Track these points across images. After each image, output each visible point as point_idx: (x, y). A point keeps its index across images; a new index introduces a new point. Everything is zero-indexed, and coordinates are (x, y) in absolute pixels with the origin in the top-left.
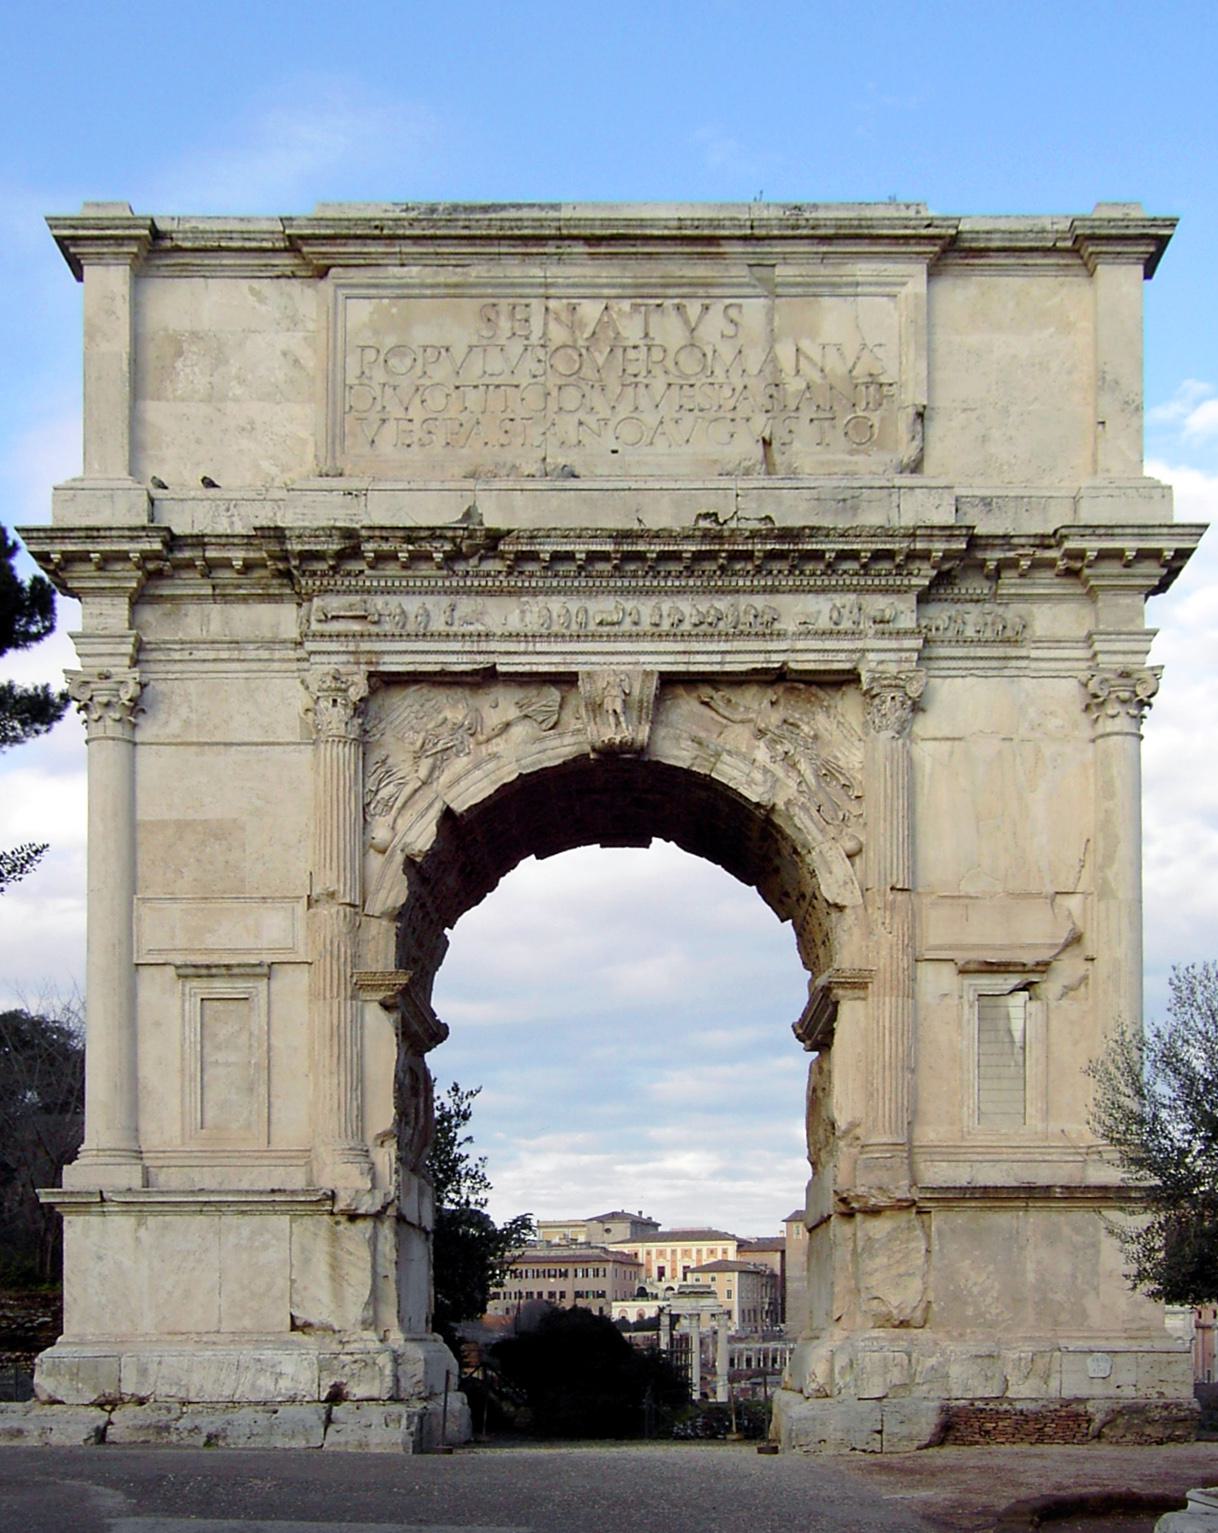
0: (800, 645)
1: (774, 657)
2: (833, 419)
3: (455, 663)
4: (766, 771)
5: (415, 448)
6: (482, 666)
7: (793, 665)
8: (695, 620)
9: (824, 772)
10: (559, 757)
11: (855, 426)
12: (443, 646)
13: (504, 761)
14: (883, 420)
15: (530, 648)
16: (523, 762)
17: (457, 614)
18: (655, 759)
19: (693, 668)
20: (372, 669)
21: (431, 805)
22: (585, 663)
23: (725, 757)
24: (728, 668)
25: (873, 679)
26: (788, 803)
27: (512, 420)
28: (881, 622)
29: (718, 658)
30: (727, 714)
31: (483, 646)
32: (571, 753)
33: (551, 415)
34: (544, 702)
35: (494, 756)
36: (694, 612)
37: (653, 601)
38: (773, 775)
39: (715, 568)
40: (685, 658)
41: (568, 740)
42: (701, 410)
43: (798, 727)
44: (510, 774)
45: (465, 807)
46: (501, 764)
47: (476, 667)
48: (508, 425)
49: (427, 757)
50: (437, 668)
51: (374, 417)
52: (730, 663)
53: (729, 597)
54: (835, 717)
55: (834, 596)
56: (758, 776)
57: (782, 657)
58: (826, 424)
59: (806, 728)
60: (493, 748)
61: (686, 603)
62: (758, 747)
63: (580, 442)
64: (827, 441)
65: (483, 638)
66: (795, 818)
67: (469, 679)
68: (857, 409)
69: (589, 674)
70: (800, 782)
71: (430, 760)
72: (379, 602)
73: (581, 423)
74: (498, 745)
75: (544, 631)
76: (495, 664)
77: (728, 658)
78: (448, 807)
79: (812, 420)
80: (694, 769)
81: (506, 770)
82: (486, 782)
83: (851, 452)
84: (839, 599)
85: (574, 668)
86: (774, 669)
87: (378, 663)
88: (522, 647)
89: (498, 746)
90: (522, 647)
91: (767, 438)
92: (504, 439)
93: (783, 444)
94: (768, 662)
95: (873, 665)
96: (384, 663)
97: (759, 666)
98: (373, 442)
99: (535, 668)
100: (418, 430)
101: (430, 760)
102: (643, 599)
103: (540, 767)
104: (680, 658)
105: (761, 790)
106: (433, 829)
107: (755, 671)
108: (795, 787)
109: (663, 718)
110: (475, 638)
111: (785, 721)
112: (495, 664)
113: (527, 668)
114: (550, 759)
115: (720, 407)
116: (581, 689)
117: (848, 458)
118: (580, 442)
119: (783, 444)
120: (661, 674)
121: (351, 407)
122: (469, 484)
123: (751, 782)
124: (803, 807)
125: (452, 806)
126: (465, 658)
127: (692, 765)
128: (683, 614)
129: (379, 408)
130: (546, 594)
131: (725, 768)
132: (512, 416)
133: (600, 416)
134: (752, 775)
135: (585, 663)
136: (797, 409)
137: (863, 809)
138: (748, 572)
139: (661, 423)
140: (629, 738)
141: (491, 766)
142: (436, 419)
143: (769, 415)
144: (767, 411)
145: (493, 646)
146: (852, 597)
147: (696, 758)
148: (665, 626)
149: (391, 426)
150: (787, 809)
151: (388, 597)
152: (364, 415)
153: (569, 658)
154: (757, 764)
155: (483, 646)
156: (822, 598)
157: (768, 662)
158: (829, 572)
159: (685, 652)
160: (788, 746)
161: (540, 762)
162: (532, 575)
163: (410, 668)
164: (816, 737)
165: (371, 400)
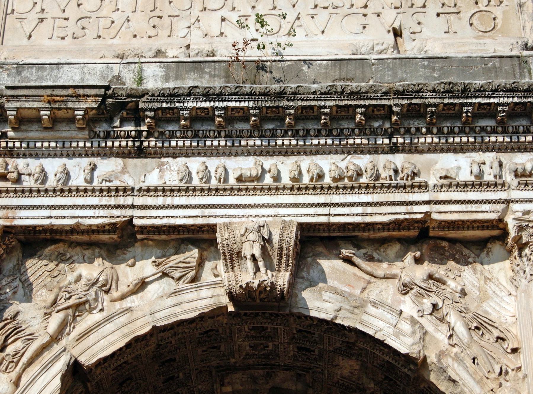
0: (443, 196)
1: (416, 208)
2: (458, 13)
3: (91, 217)
4: (413, 322)
5: (69, 39)
6: (118, 219)
7: (435, 216)
8: (336, 174)
9: (475, 324)
10: (195, 309)
11: (479, 19)
12: (80, 201)
13: (135, 315)
14: (504, 12)
15: (169, 201)
16: (156, 315)
17: (96, 174)
18: (295, 311)
19: (334, 220)
20: (8, 224)
21: (57, 357)
22: (223, 217)
23: (370, 309)
24: (368, 219)
25: (521, 229)
26: (441, 354)
27: (160, 17)
28: (523, 175)
29: (359, 210)
30: (369, 269)
31: (121, 201)
32: (207, 307)
33: (196, 12)
34: (182, 259)
35: (129, 310)
36: (333, 167)
37: (291, 160)
38: (422, 327)
39: (352, 126)
40: (325, 210)
41: (205, 293)
42: (336, 7)
43: (444, 283)
44: (142, 327)
45: (94, 361)
46: (134, 317)
47: (114, 221)
48: (156, 21)
49: (58, 312)
50: (71, 222)
51: (34, 17)
52: (371, 214)
53: (368, 156)
54: (482, 273)
55: (474, 154)
56: (406, 327)
57: (425, 208)
58: (453, 17)
59: (452, 284)
60: (127, 303)
61: (326, 161)
62: (404, 302)
63: (222, 34)
64: (454, 29)
65: (121, 193)
66: (449, 370)
67: (105, 237)
68: (480, 5)
69: (227, 225)
70: (451, 336)
71: (61, 315)
72: (21, 163)
73: (223, 20)
74: (133, 301)
75: (183, 185)
76: (132, 218)
77: (369, 210)
78: (76, 361)
79: (438, 15)
80: (338, 321)
81: (139, 323)
82: (117, 335)
83: (478, 38)
84: (478, 156)
85: (212, 221)
86: (417, 221)
87: (13, 218)
88: (160, 201)
89: (133, 301)
90: (160, 201)
91: (396, 25)
92: (152, 32)
93: (414, 33)
94: (410, 213)
95: (520, 215)
96: (20, 218)
97: (402, 217)
98: (30, 36)
99: (172, 222)
100: (72, 27)
101: (61, 315)
102: (281, 158)
103: (175, 320)
104: (320, 210)
105: (409, 341)
106: (57, 382)
107: (397, 224)
108: (446, 341)
109: (304, 274)
110: (113, 193)
111: (431, 277)
112: (132, 218)
113: (165, 222)
114: (185, 312)
115: (352, 5)
116: (219, 240)
117: (475, 41)
118: (222, 34)
119: (414, 33)
120: (301, 226)
121: (13, 10)
122: (118, 60)
123: (399, 333)
124: (457, 358)
125: (78, 359)
126: (102, 212)
127: (336, 317)
128: (322, 171)
129: (38, 8)
130: (187, 155)
131: (371, 320)
132: (160, 15)
133: (241, 13)
134: (399, 326)
135: (223, 217)
136: (424, 6)
137: (520, 360)
138: (386, 130)
139: (298, 18)
140: (268, 282)
141: (123, 319)
142: (90, 18)
143: (398, 11)
144: (396, 8)
145: (129, 201)
146: (493, 155)
147: (340, 310)
148: (306, 180)
149: (47, 25)
150: (439, 361)
151: (30, 160)
152: (23, 16)
153: (207, 212)
154: (404, 315)
155: (121, 201)
156: (460, 156)
157: (410, 213)
158: (467, 130)
159: (325, 205)
160: (434, 299)
161: (175, 315)
162: (172, 135)
163: (46, 222)
164: (463, 293)
165: (33, 4)
